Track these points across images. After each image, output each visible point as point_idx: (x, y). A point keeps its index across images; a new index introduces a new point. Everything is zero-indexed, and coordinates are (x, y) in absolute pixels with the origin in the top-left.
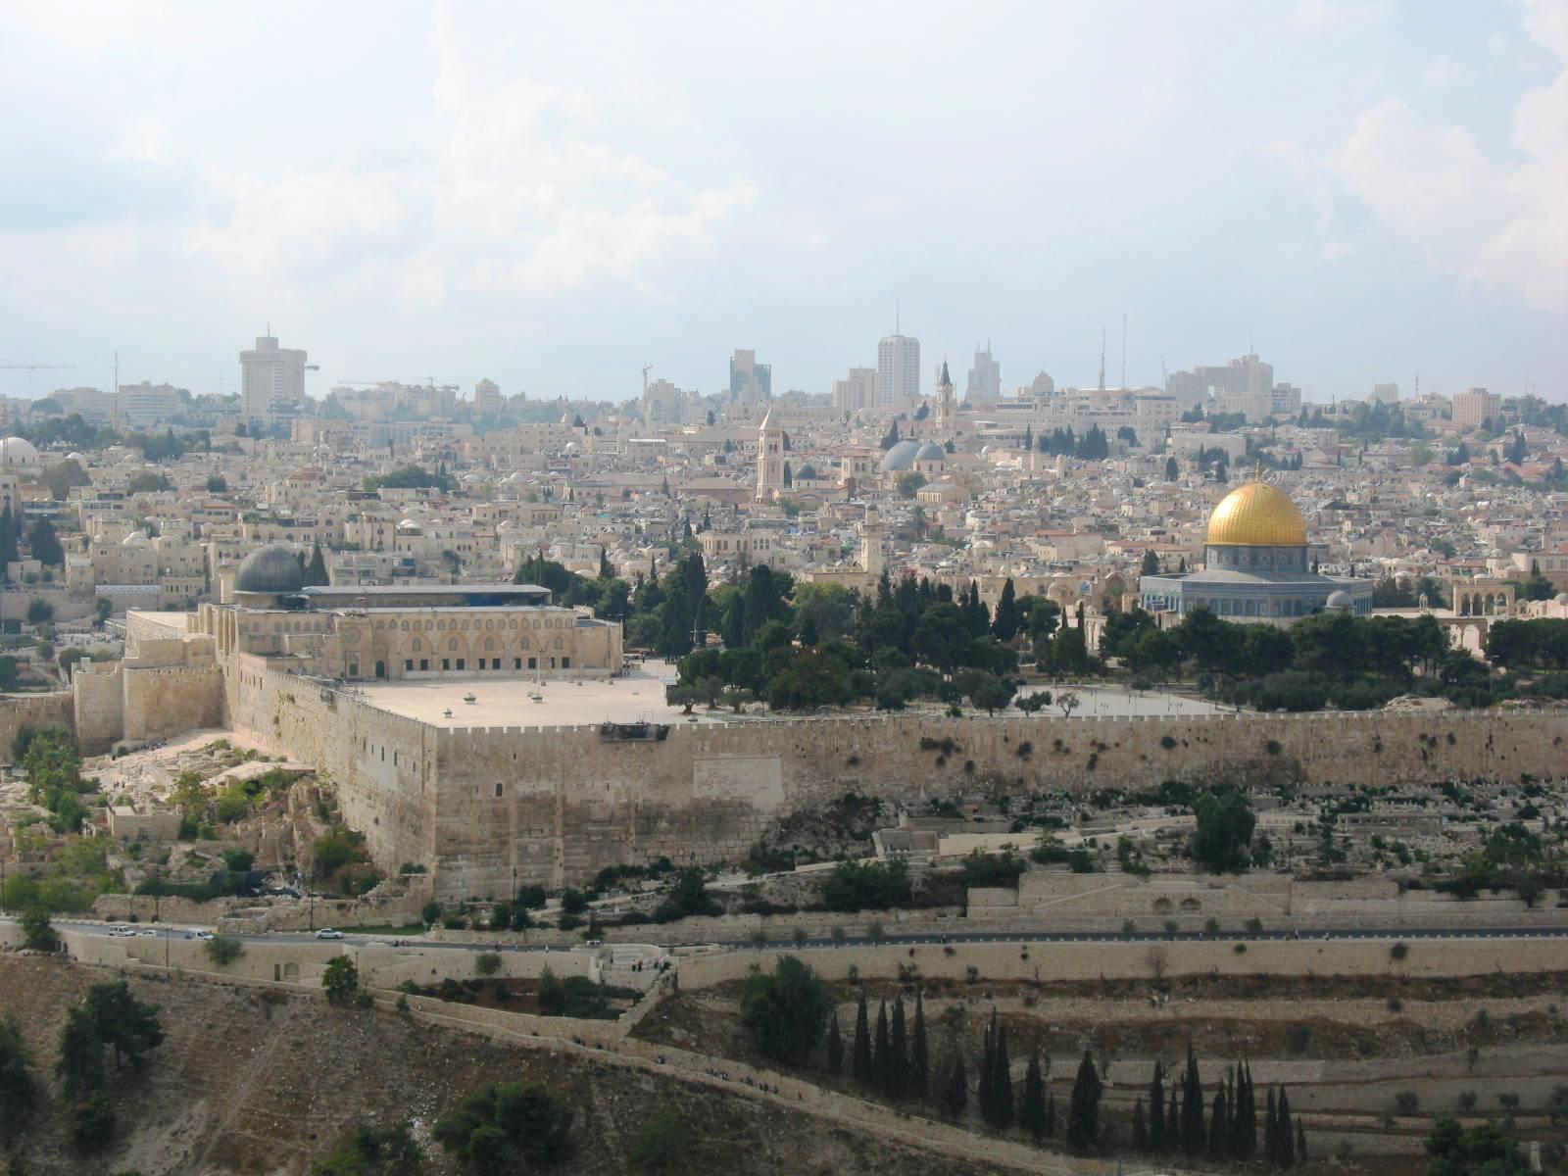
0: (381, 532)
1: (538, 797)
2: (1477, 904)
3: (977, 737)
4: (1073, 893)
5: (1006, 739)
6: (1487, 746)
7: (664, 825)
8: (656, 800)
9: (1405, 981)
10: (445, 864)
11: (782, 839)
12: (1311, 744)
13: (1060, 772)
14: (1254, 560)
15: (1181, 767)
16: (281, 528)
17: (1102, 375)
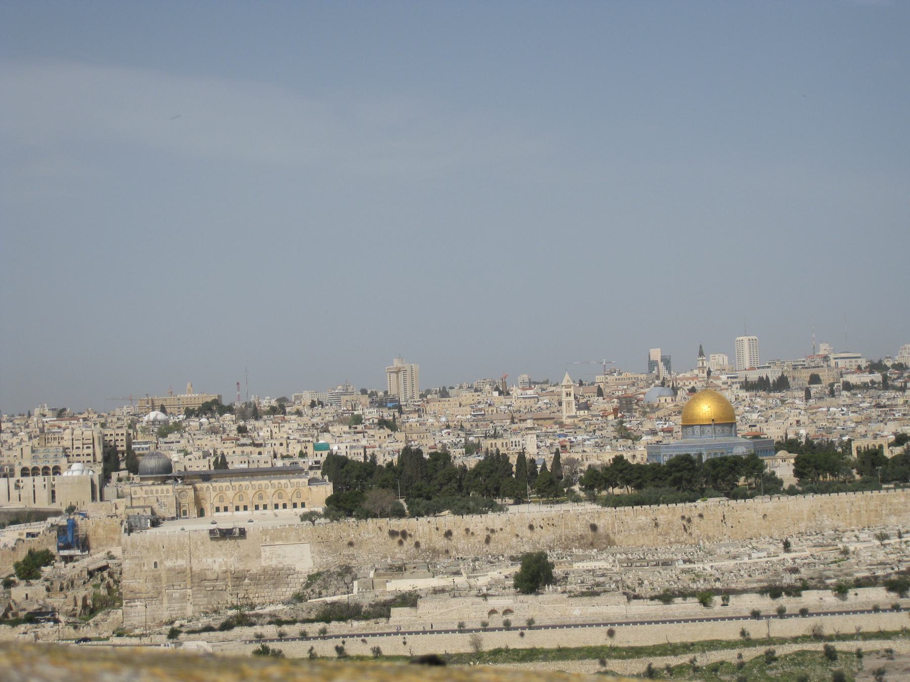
0: (306, 448)
1: (177, 568)
2: (672, 606)
3: (420, 528)
4: (447, 608)
5: (437, 529)
6: (722, 521)
7: (247, 581)
8: (241, 568)
9: (614, 649)
10: (129, 604)
11: (307, 586)
12: (616, 525)
13: (470, 545)
14: (702, 432)
15: (540, 539)
16: (255, 448)
17: (814, 347)
